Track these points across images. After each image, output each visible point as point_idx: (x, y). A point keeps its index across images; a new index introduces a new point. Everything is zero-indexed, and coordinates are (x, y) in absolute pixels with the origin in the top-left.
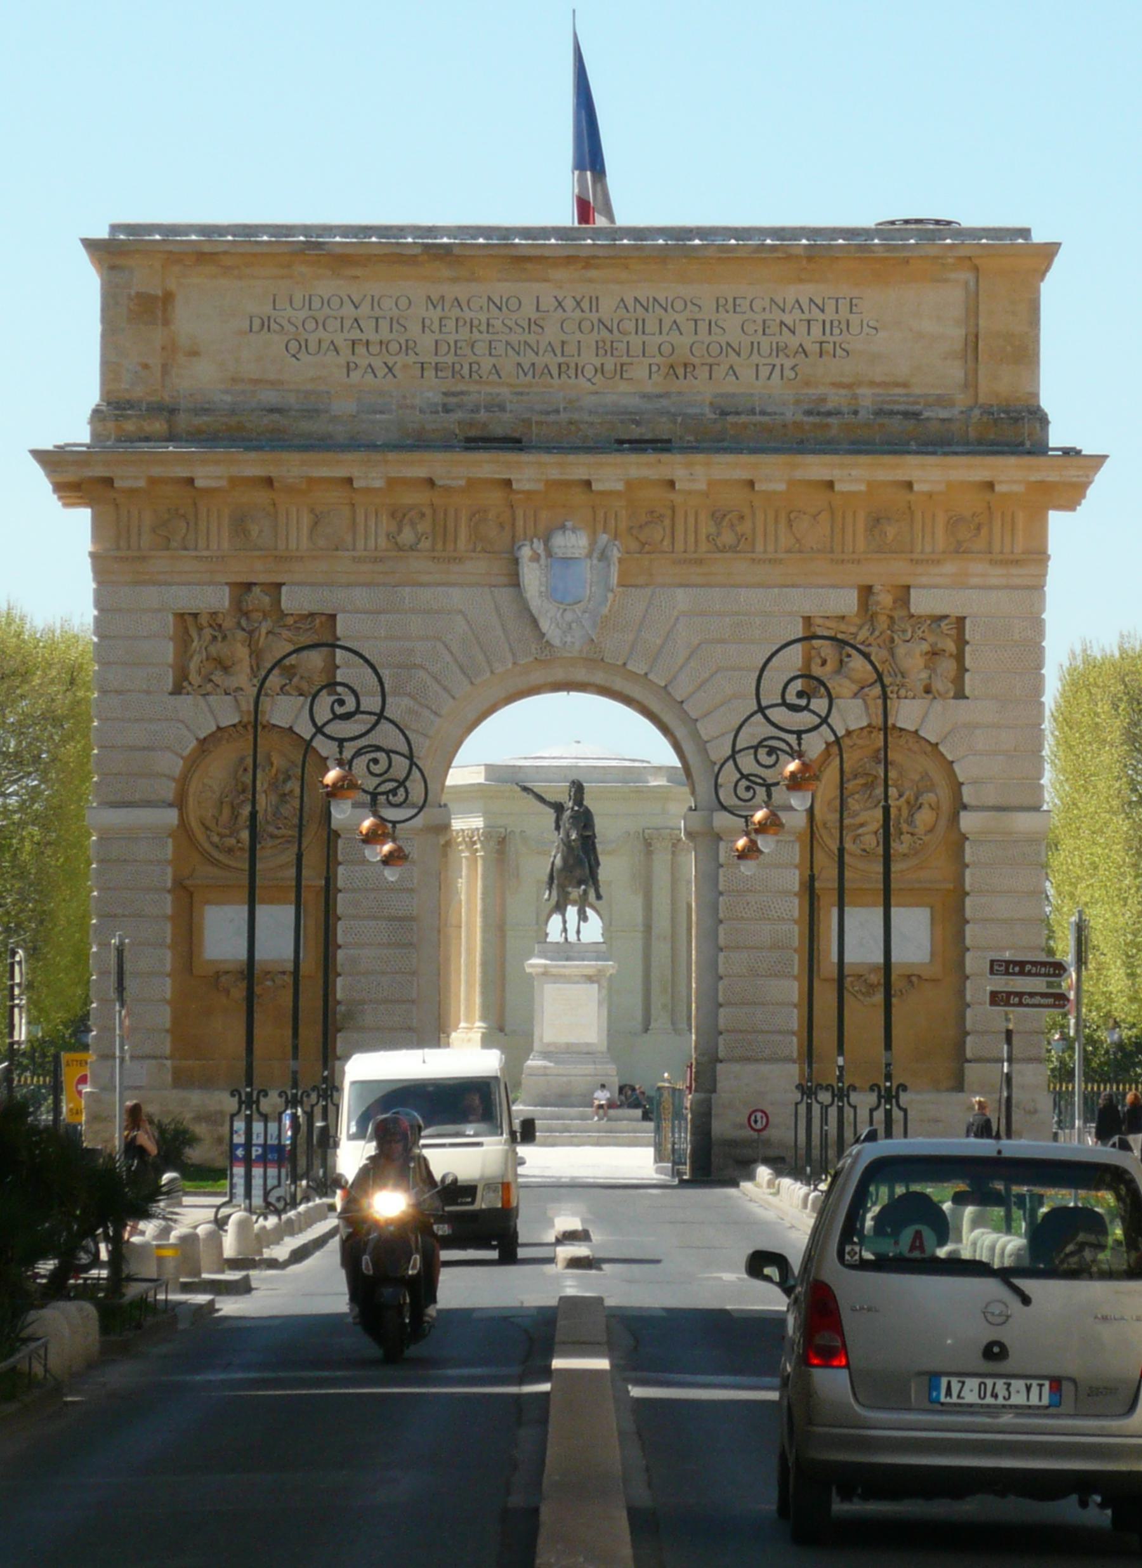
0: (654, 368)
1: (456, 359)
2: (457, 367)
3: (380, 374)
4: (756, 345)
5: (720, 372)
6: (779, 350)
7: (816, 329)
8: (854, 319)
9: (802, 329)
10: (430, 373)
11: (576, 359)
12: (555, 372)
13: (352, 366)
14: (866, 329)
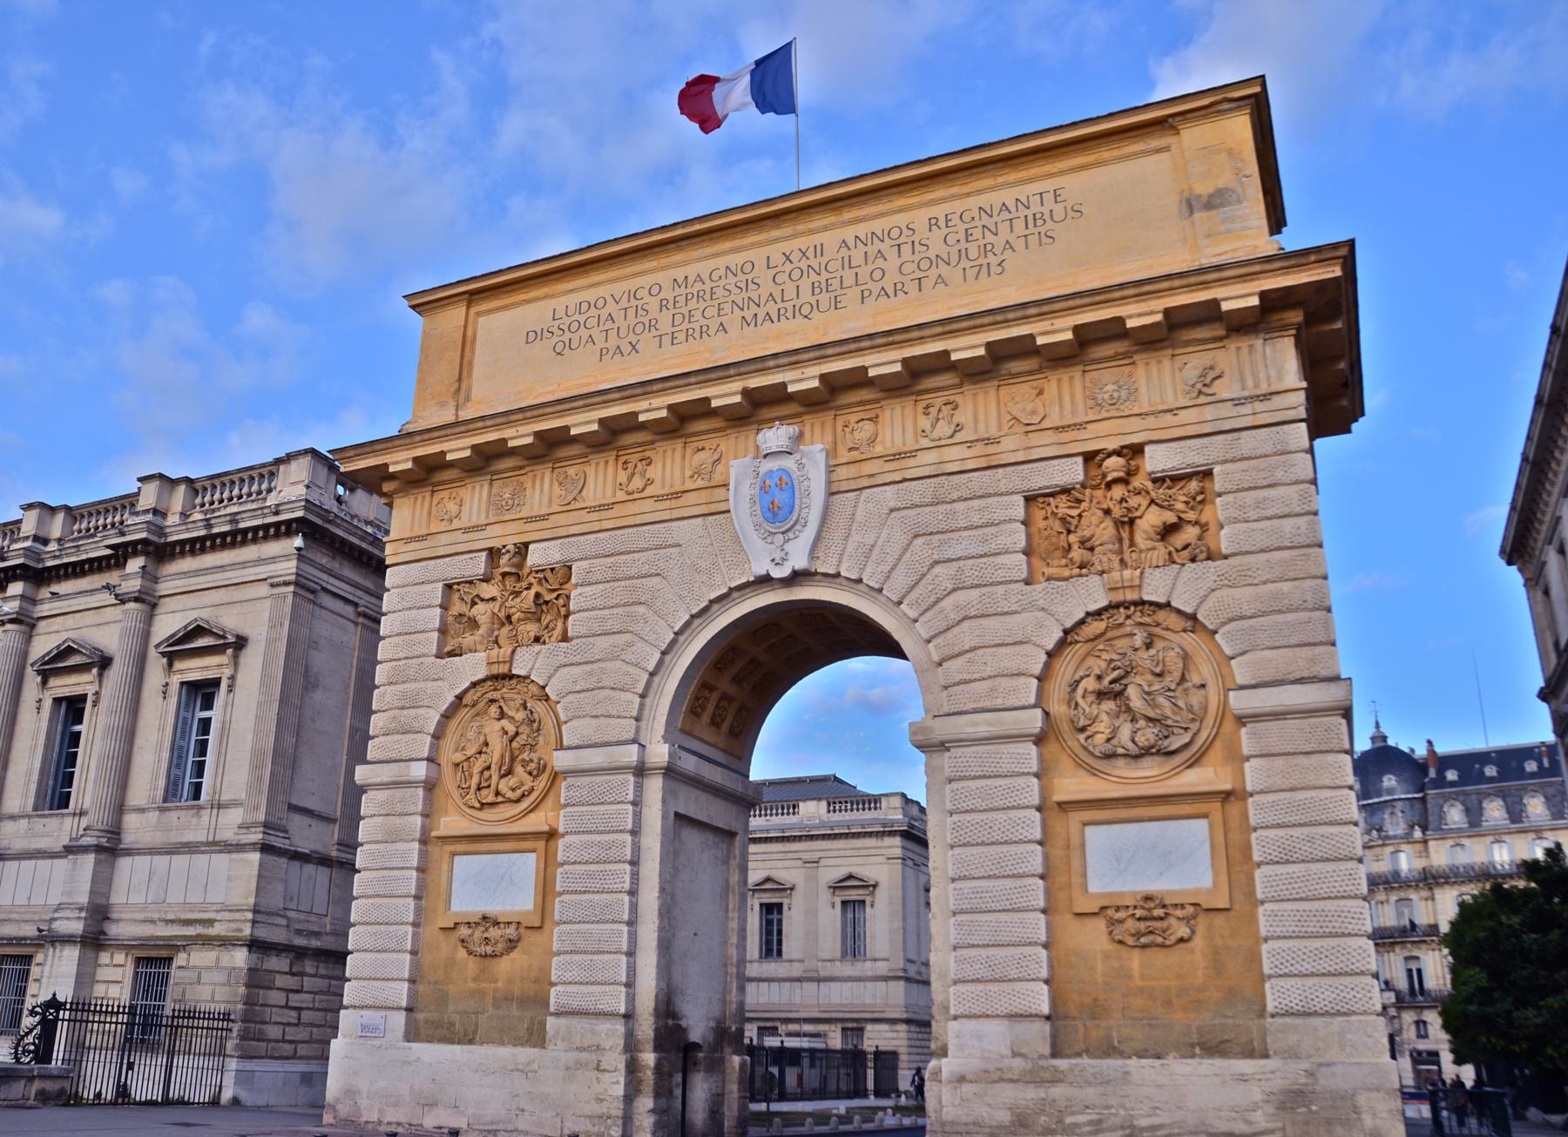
0: (866, 293)
1: (692, 325)
2: (691, 332)
3: (626, 348)
4: (963, 251)
6: (986, 250)
7: (1019, 225)
8: (1059, 212)
9: (1004, 228)
10: (667, 340)
11: (792, 303)
12: (775, 319)
13: (604, 351)
14: (1071, 214)
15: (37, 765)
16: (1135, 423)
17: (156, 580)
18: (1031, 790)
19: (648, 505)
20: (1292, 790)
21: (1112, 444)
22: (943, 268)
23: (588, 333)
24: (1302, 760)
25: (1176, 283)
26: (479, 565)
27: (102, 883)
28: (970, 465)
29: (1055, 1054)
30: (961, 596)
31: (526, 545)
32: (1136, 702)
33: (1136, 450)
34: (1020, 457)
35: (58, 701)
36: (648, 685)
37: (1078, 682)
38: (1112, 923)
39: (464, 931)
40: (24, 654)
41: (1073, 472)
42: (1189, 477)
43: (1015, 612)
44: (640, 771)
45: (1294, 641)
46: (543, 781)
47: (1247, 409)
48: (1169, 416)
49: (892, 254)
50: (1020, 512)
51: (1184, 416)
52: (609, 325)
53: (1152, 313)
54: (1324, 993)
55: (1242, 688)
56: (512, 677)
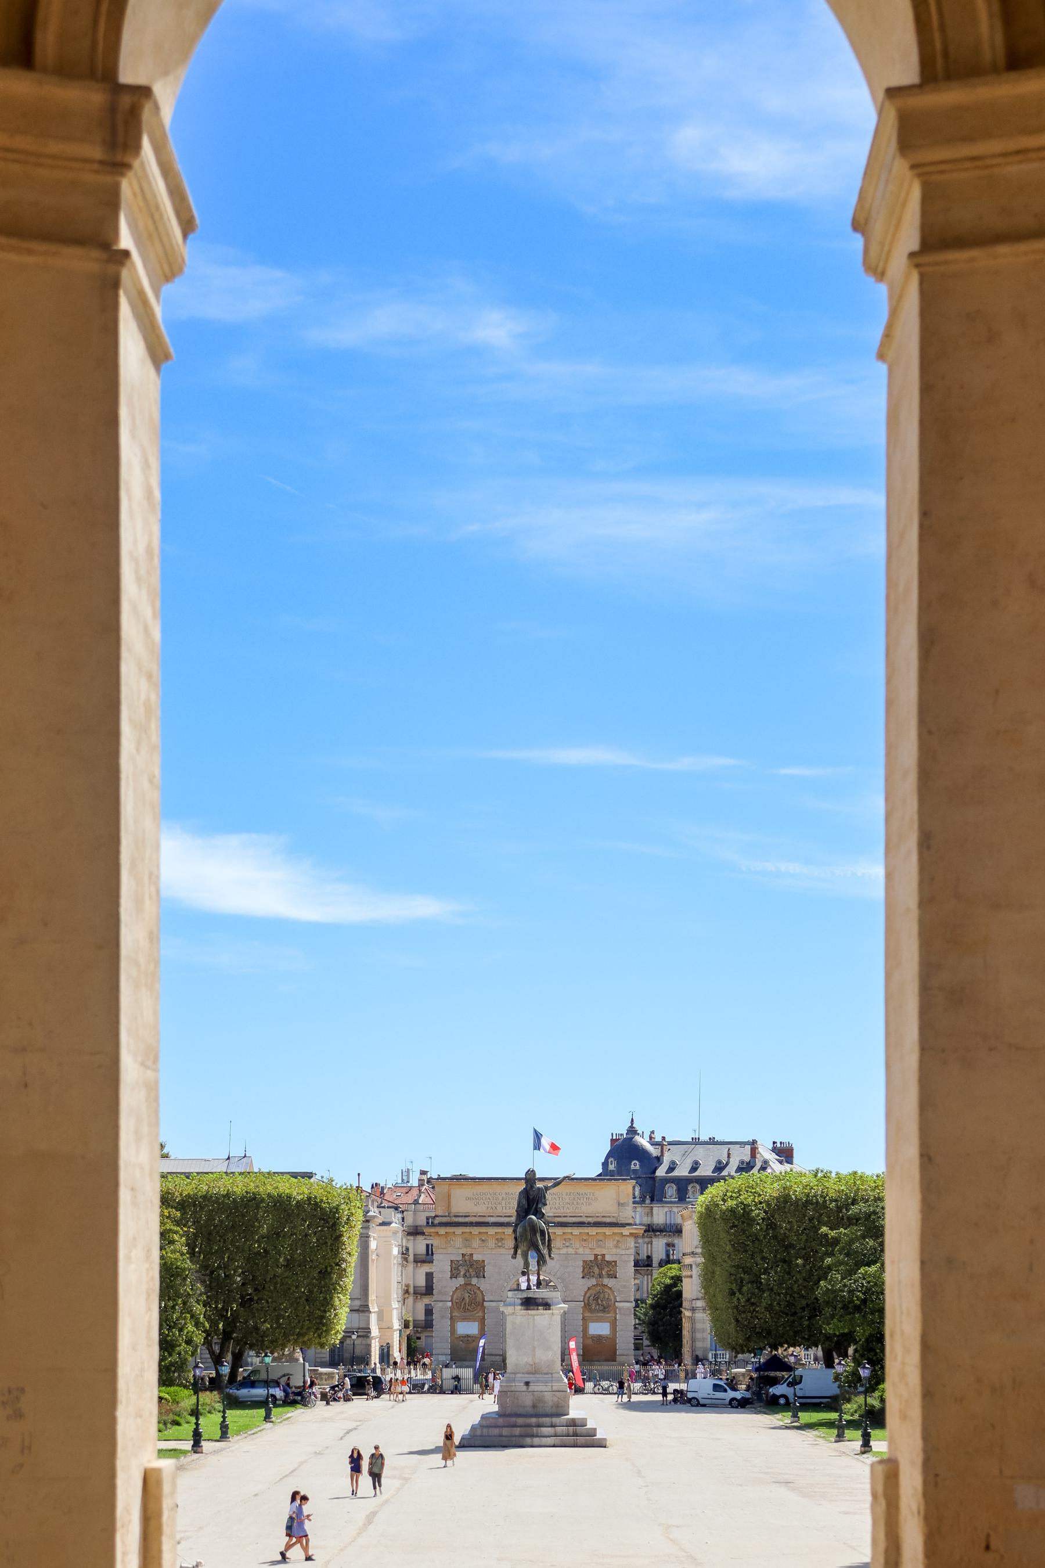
10: (504, 1208)
22: (569, 1206)
23: (483, 1201)
26: (460, 1258)
28: (573, 1253)
29: (583, 1361)
31: (472, 1254)
32: (600, 1302)
34: (583, 1253)
37: (589, 1298)
38: (593, 1340)
39: (462, 1338)
42: (613, 1261)
46: (479, 1307)
47: (624, 1251)
49: (558, 1199)
54: (625, 1352)
56: (470, 1284)
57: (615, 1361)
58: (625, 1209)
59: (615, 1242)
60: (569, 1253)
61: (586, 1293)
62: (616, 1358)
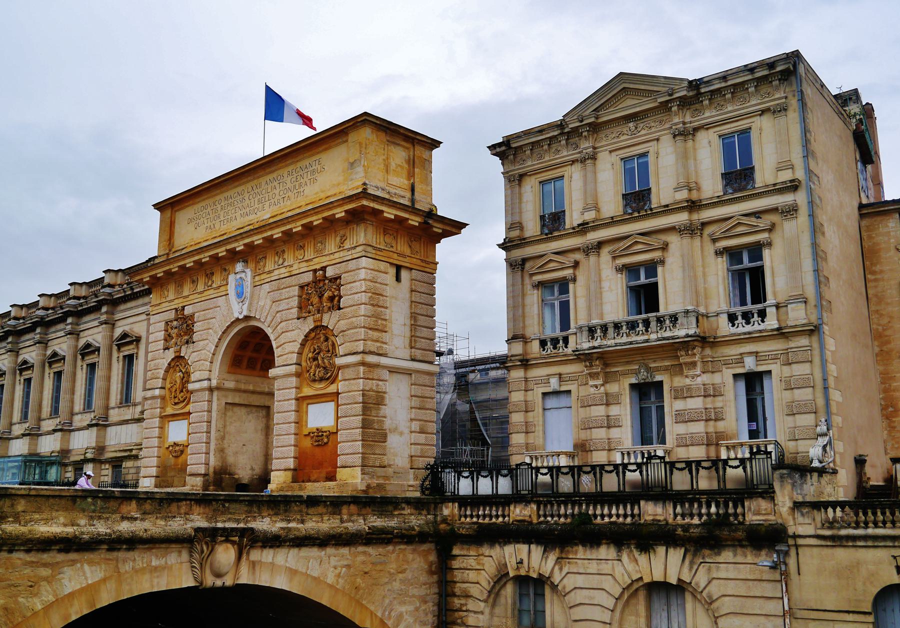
5: (285, 199)
6: (300, 186)
15: (83, 392)
16: (324, 259)
17: (113, 314)
18: (293, 393)
19: (212, 292)
20: (349, 392)
21: (318, 267)
24: (352, 381)
25: (323, 208)
27: (101, 438)
29: (292, 482)
30: (283, 324)
33: (324, 269)
34: (297, 272)
35: (124, 357)
36: (212, 358)
38: (312, 437)
40: (112, 336)
41: (309, 277)
43: (293, 330)
44: (211, 390)
45: (354, 339)
47: (350, 253)
48: (332, 257)
49: (277, 186)
50: (296, 293)
51: (337, 255)
52: (208, 217)
53: (319, 219)
54: (349, 460)
55: (342, 356)
57: (336, 480)
58: (356, 173)
59: (338, 239)
60: (282, 276)
61: (303, 345)
62: (335, 472)
